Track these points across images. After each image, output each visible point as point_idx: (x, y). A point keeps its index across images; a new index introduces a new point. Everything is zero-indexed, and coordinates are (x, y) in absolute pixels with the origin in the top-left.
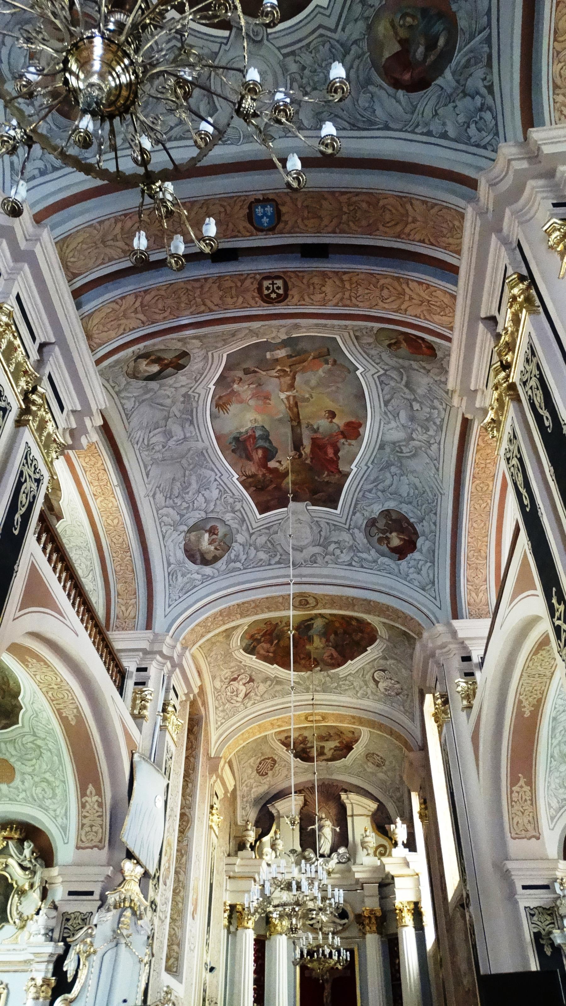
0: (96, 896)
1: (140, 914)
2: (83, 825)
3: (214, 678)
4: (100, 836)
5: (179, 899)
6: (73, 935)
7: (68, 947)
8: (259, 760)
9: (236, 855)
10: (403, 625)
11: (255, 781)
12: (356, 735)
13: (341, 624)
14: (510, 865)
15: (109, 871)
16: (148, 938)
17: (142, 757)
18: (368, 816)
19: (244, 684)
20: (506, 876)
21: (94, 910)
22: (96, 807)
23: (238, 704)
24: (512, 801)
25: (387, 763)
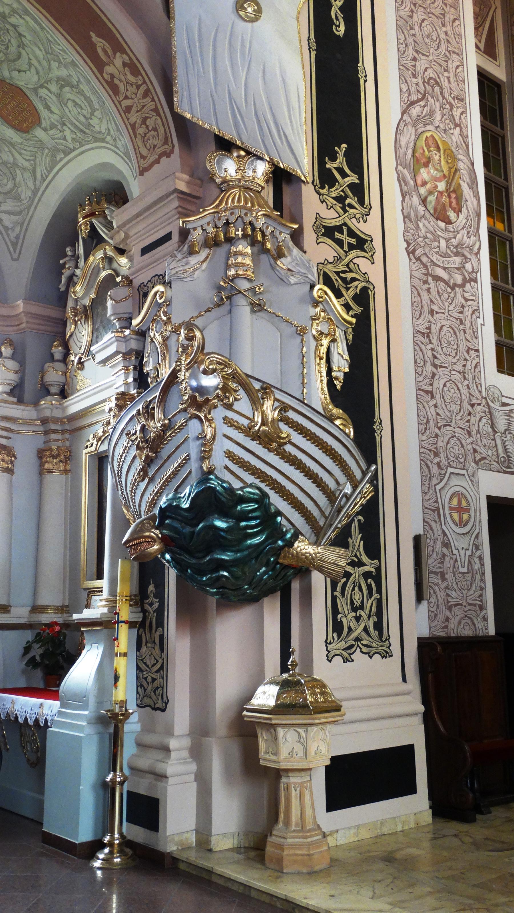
22: (131, 78)
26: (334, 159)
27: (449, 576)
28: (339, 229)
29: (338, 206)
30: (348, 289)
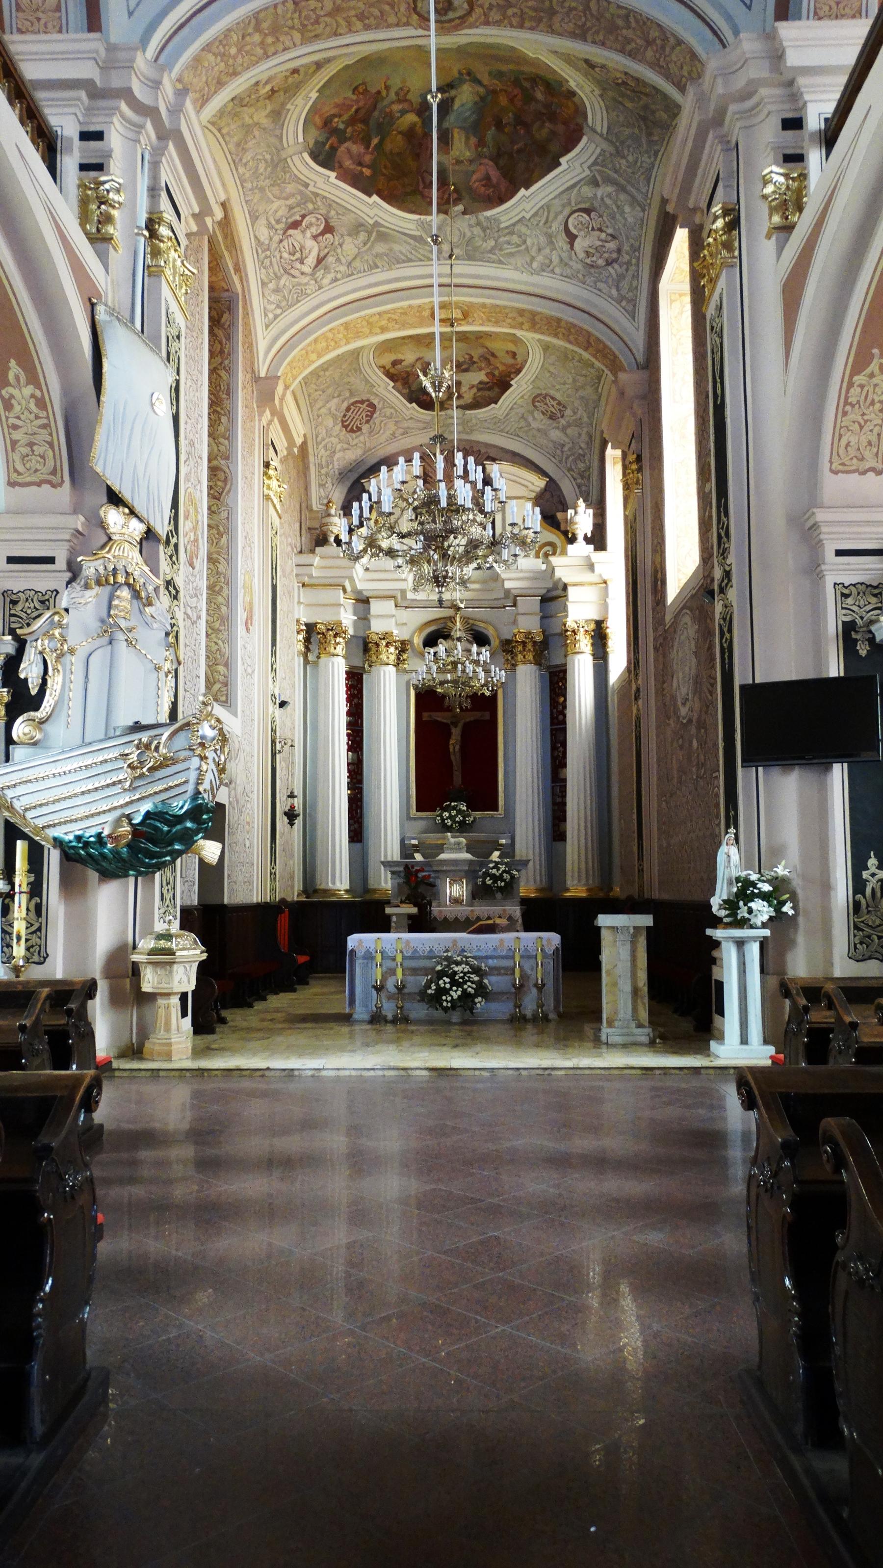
0: (61, 563)
1: (148, 598)
2: (14, 443)
3: (254, 217)
4: (50, 463)
5: (220, 599)
6: (28, 625)
7: (21, 644)
8: (345, 405)
9: (312, 551)
10: (655, 65)
11: (340, 441)
12: (519, 359)
13: (511, 100)
14: (821, 516)
15: (79, 522)
16: (167, 634)
17: (111, 312)
18: (529, 499)
19: (315, 237)
20: (808, 534)
21: (60, 584)
23: (305, 280)
24: (846, 403)
25: (568, 412)
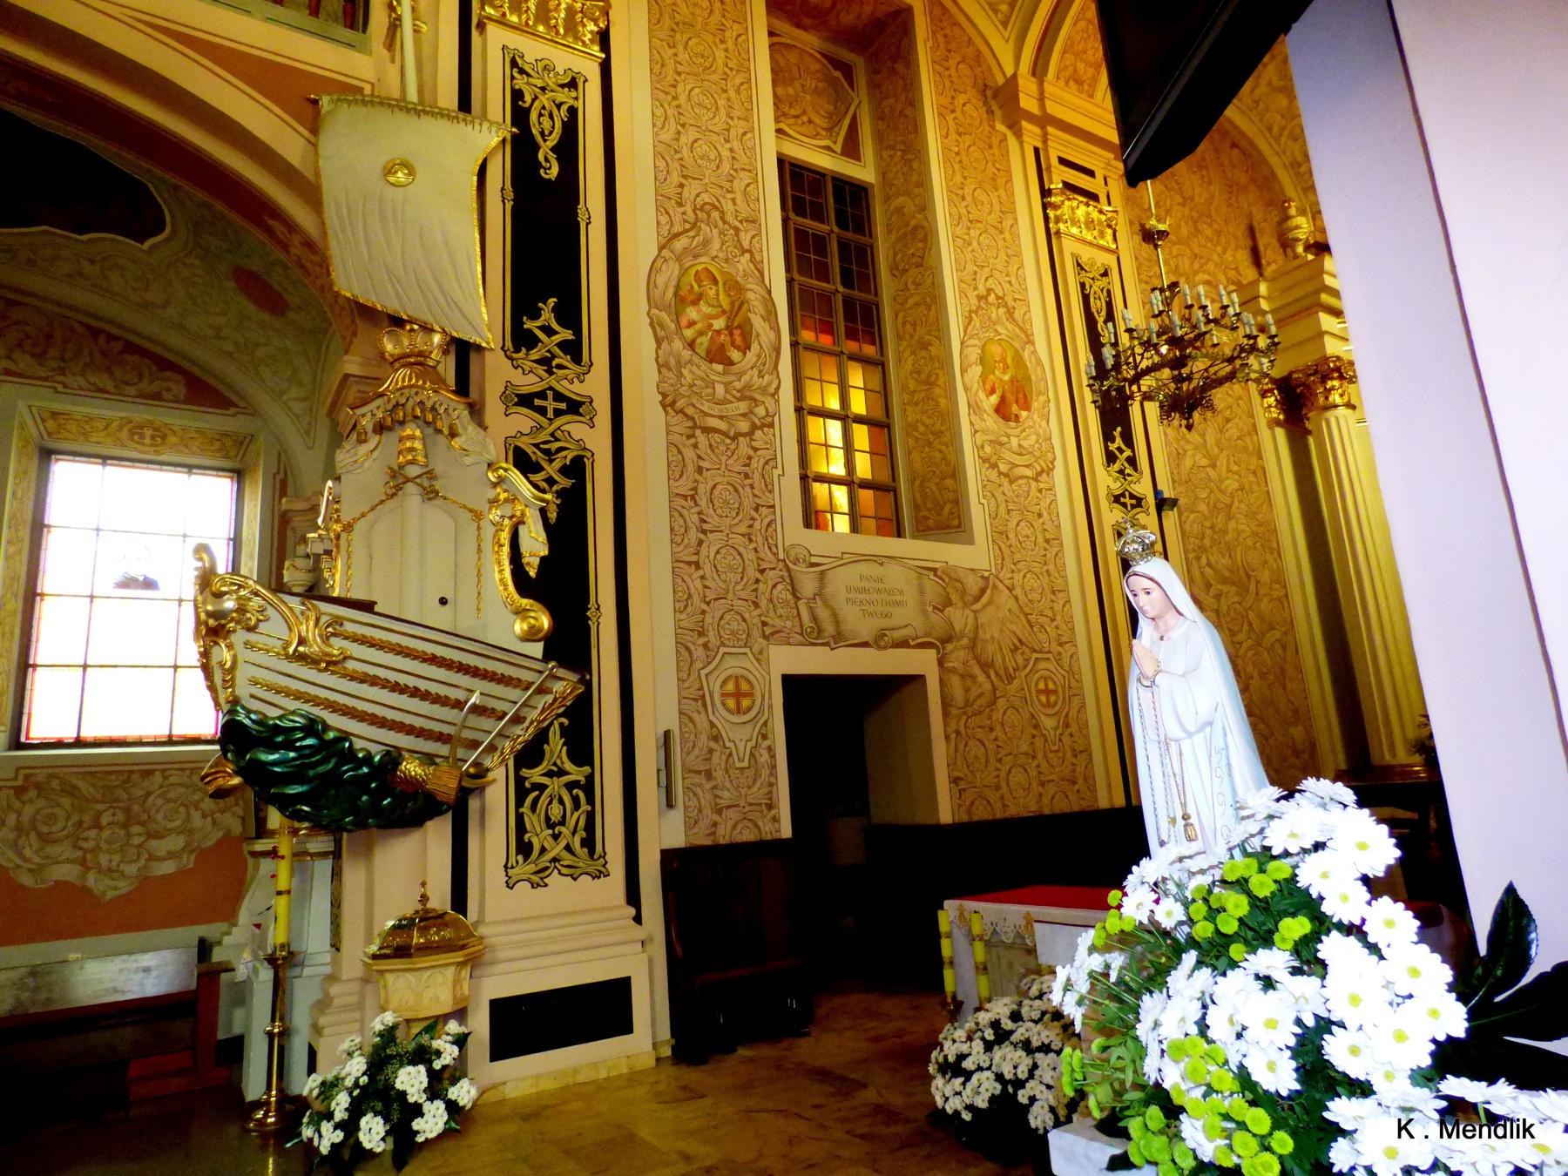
26: (536, 315)
27: (719, 775)
28: (542, 395)
29: (541, 370)
30: (551, 461)
